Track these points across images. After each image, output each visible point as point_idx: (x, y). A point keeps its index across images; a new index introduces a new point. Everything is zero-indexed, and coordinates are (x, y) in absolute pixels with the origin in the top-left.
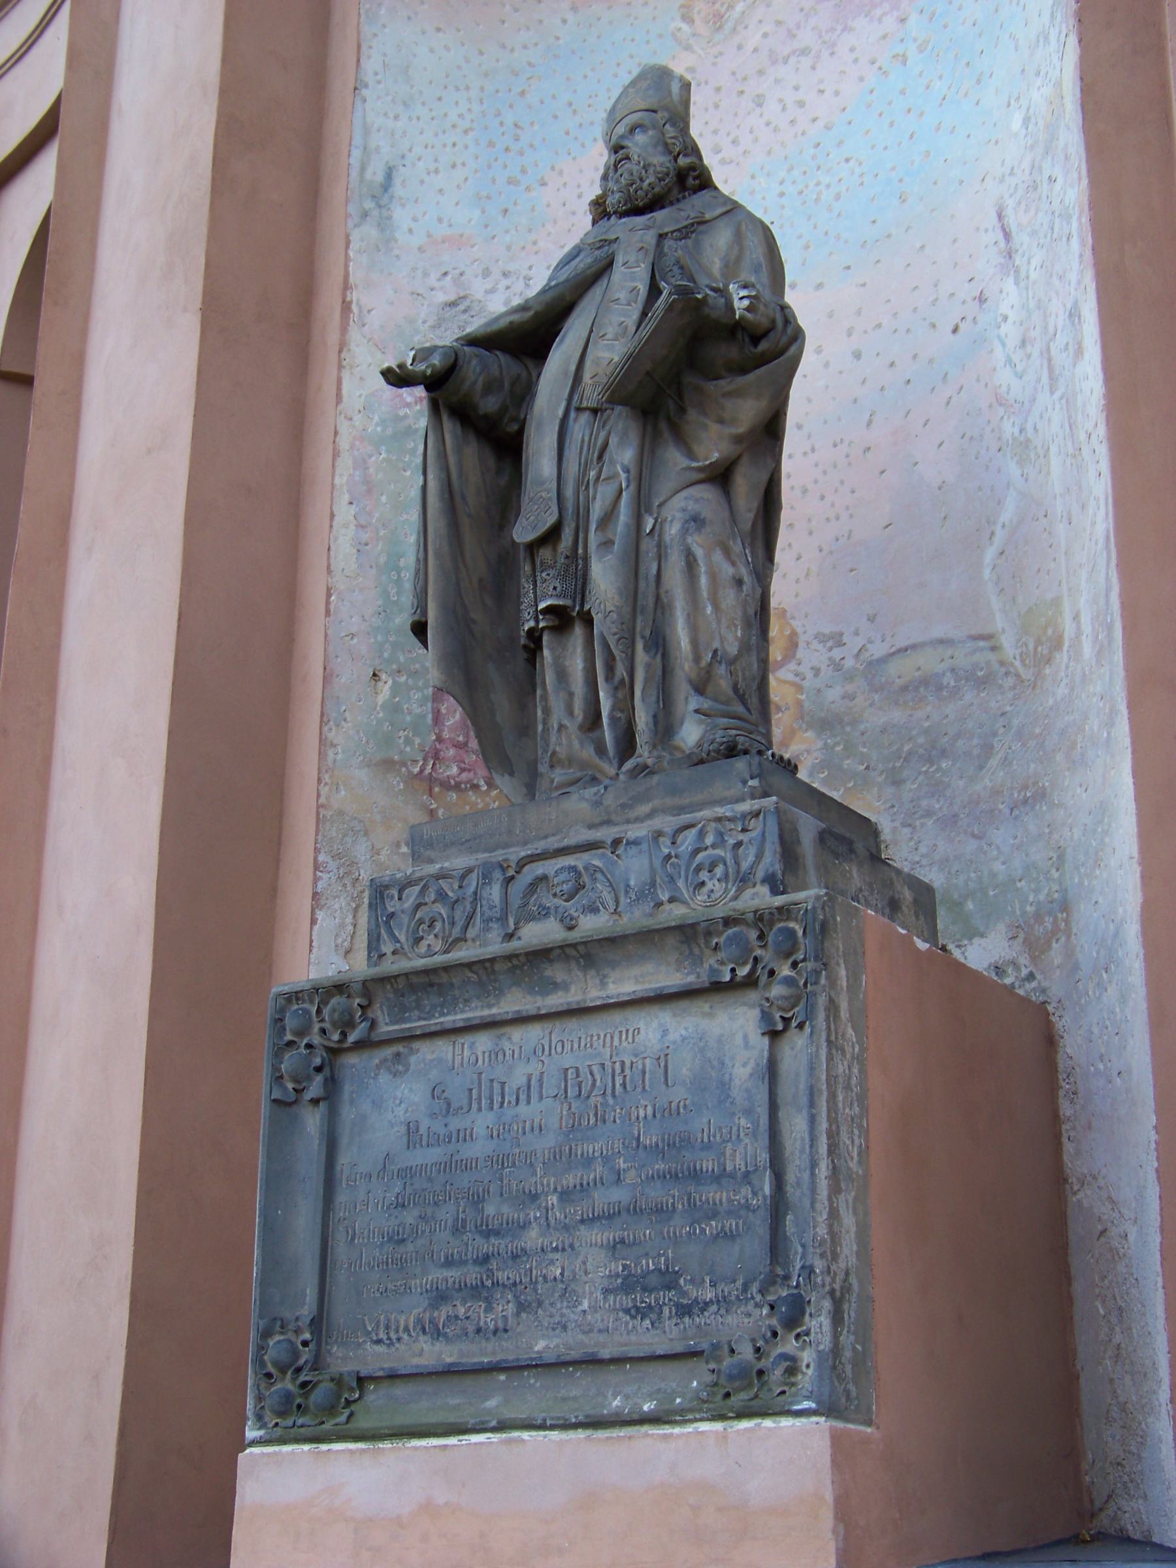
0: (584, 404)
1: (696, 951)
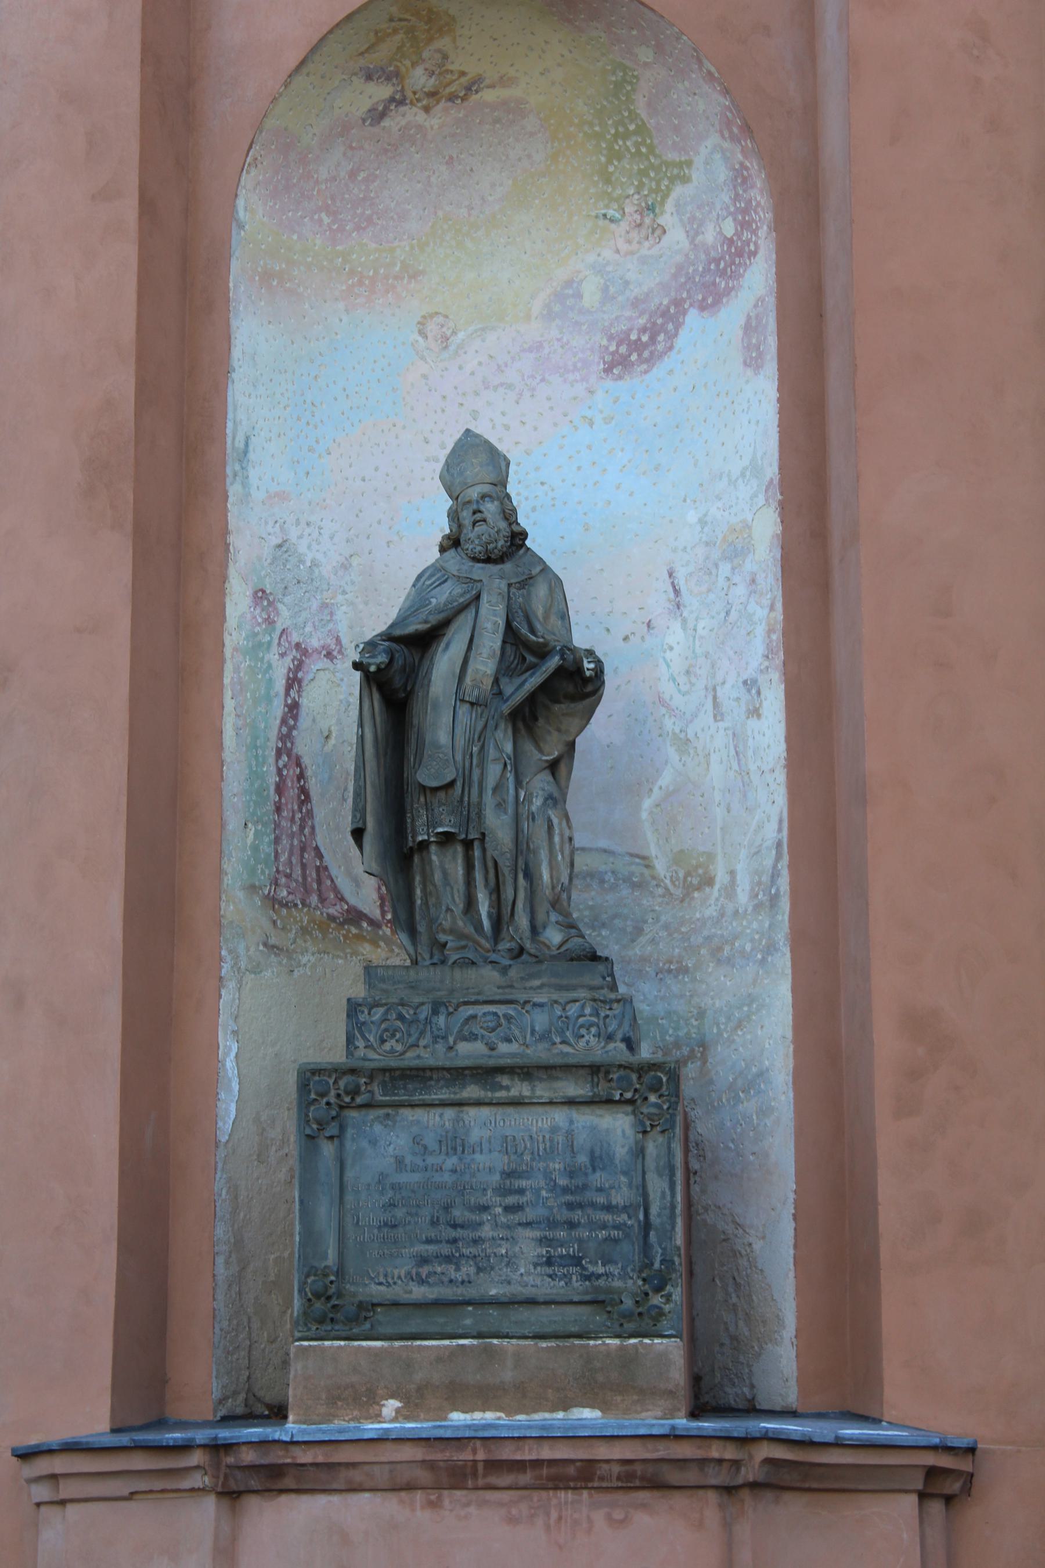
0: (467, 699)
1: (596, 1080)
